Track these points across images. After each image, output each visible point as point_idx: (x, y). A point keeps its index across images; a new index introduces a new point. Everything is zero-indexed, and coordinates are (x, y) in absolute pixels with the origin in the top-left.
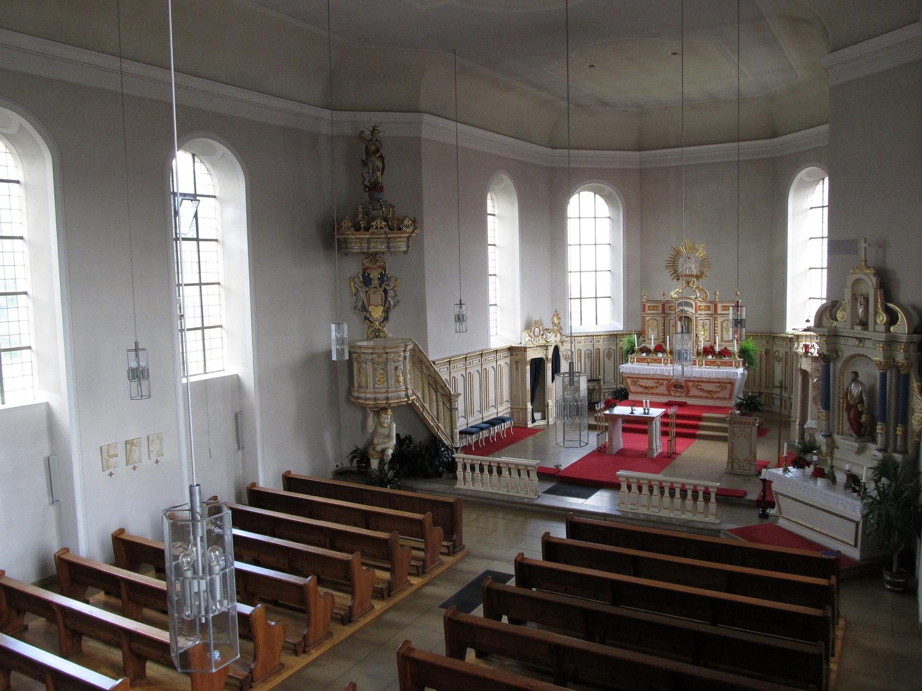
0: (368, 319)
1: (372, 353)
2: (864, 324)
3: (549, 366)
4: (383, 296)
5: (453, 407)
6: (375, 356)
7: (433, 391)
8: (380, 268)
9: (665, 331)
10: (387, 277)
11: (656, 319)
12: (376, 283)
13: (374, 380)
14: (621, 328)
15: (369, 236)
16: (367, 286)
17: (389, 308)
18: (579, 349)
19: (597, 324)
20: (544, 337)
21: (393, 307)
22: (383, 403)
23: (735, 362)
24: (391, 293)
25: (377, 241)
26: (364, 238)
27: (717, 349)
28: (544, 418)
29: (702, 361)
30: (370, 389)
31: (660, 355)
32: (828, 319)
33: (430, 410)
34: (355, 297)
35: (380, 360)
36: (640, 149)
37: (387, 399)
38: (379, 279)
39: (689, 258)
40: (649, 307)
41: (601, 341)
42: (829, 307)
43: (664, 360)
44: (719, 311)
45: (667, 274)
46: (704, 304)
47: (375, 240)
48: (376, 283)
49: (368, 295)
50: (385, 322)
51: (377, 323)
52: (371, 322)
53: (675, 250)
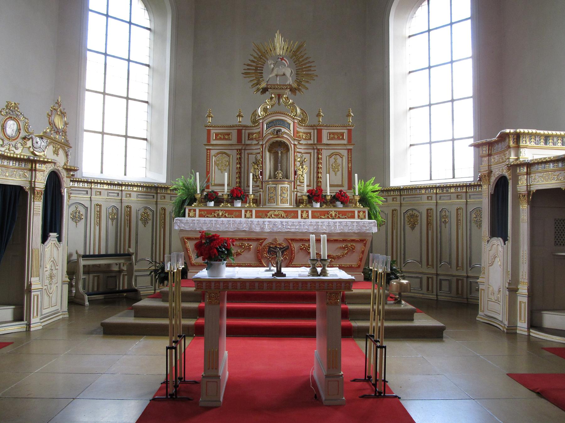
9: (241, 170)
18: (97, 205)
27: (329, 192)
28: (18, 317)
29: (307, 212)
31: (238, 204)
39: (282, 59)
41: (134, 195)
43: (246, 211)
44: (325, 140)
46: (301, 130)
53: (259, 49)
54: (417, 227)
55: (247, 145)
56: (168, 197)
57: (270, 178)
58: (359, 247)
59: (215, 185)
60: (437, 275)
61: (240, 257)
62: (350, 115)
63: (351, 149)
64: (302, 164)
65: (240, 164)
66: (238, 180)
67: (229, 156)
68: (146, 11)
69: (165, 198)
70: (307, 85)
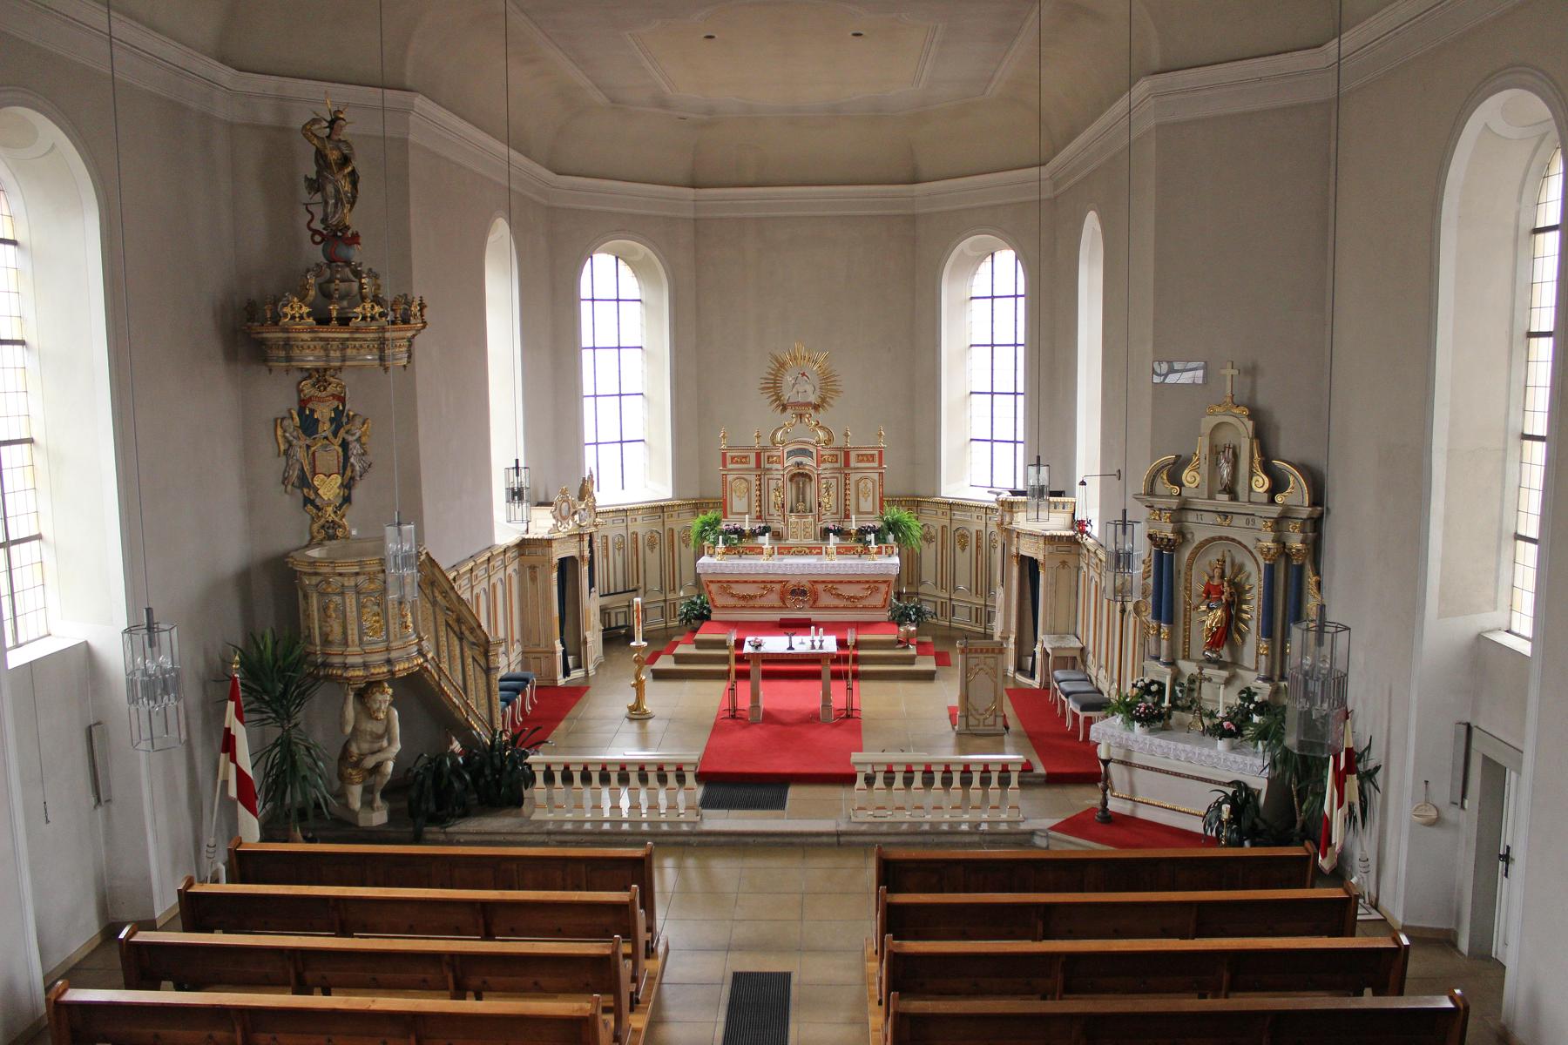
0: (312, 502)
1: (357, 574)
2: (1231, 491)
3: (584, 570)
4: (341, 453)
5: (492, 666)
6: (361, 579)
7: (455, 638)
8: (334, 398)
10: (348, 415)
11: (744, 479)
12: (325, 428)
13: (360, 626)
14: (669, 495)
15: (347, 335)
16: (310, 436)
17: (352, 478)
19: (623, 488)
20: (577, 517)
21: (361, 476)
22: (384, 673)
23: (886, 548)
24: (355, 449)
25: (361, 346)
26: (334, 339)
30: (353, 646)
32: (1164, 484)
33: (451, 674)
34: (283, 459)
35: (372, 586)
36: (694, 185)
37: (389, 662)
38: (332, 420)
39: (803, 374)
40: (733, 458)
41: (639, 518)
42: (1169, 464)
44: (853, 463)
45: (765, 400)
46: (827, 452)
47: (357, 344)
48: (325, 428)
49: (310, 452)
50: (344, 507)
51: (330, 509)
52: (318, 509)
53: (777, 360)
54: (968, 548)
55: (768, 469)
56: (675, 514)
57: (791, 511)
58: (883, 588)
59: (732, 513)
60: (986, 606)
61: (763, 598)
62: (881, 434)
63: (882, 473)
64: (827, 490)
65: (760, 490)
66: (758, 509)
67: (746, 480)
68: (635, 279)
69: (672, 516)
70: (831, 402)
